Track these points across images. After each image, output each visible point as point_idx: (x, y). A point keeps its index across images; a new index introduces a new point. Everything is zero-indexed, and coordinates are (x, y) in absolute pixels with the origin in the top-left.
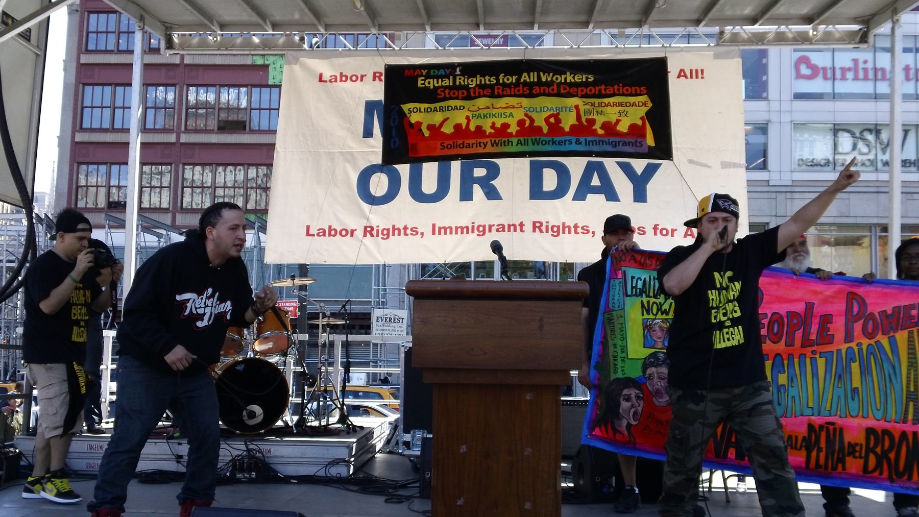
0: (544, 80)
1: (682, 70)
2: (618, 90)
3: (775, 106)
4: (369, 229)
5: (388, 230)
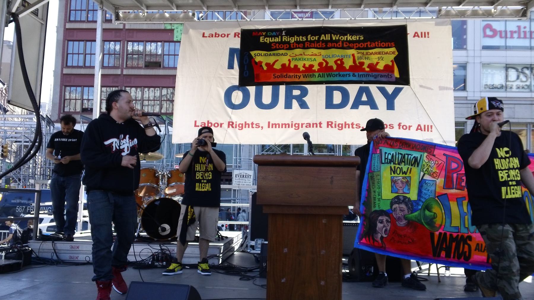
0: (334, 39)
1: (416, 33)
2: (378, 45)
3: (471, 53)
4: (231, 123)
5: (242, 124)
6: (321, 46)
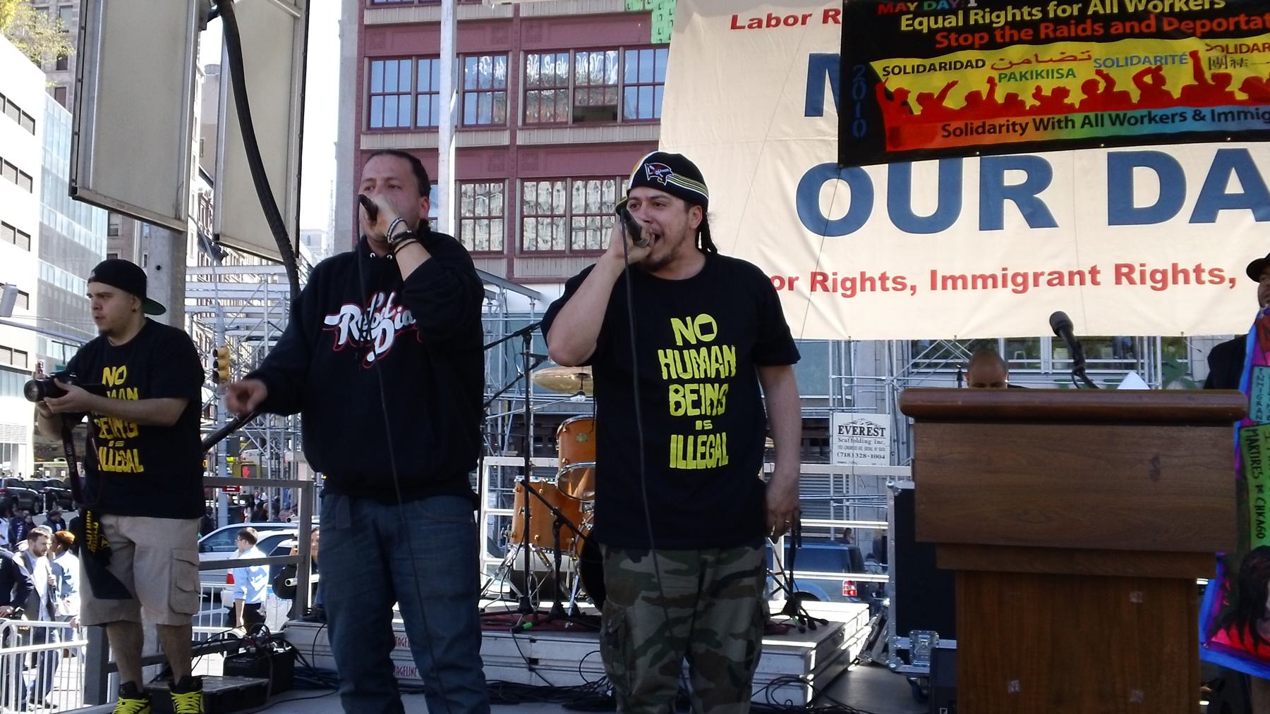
0: (1131, 9)
4: (819, 278)
5: (853, 280)
6: (1089, 33)
